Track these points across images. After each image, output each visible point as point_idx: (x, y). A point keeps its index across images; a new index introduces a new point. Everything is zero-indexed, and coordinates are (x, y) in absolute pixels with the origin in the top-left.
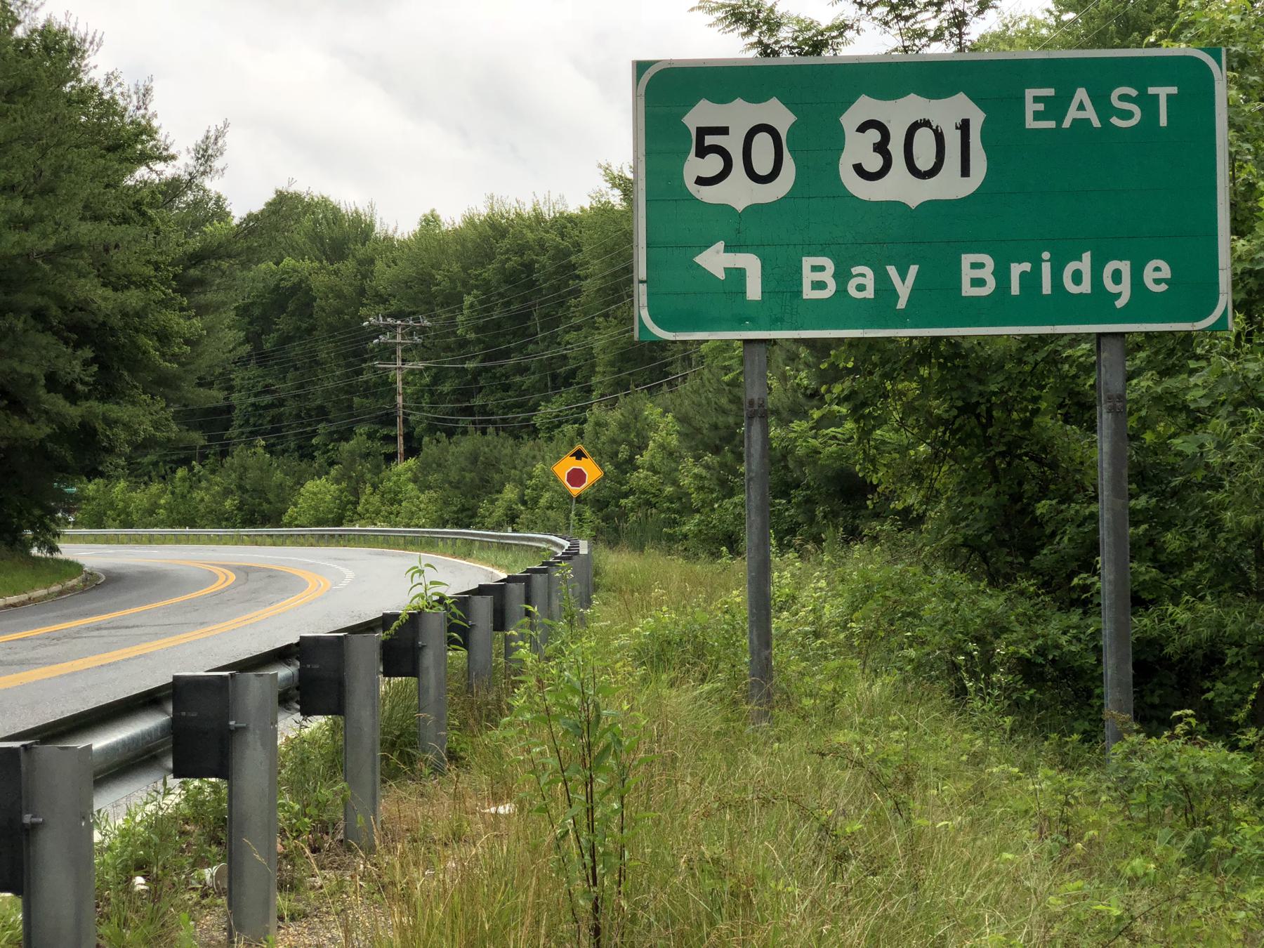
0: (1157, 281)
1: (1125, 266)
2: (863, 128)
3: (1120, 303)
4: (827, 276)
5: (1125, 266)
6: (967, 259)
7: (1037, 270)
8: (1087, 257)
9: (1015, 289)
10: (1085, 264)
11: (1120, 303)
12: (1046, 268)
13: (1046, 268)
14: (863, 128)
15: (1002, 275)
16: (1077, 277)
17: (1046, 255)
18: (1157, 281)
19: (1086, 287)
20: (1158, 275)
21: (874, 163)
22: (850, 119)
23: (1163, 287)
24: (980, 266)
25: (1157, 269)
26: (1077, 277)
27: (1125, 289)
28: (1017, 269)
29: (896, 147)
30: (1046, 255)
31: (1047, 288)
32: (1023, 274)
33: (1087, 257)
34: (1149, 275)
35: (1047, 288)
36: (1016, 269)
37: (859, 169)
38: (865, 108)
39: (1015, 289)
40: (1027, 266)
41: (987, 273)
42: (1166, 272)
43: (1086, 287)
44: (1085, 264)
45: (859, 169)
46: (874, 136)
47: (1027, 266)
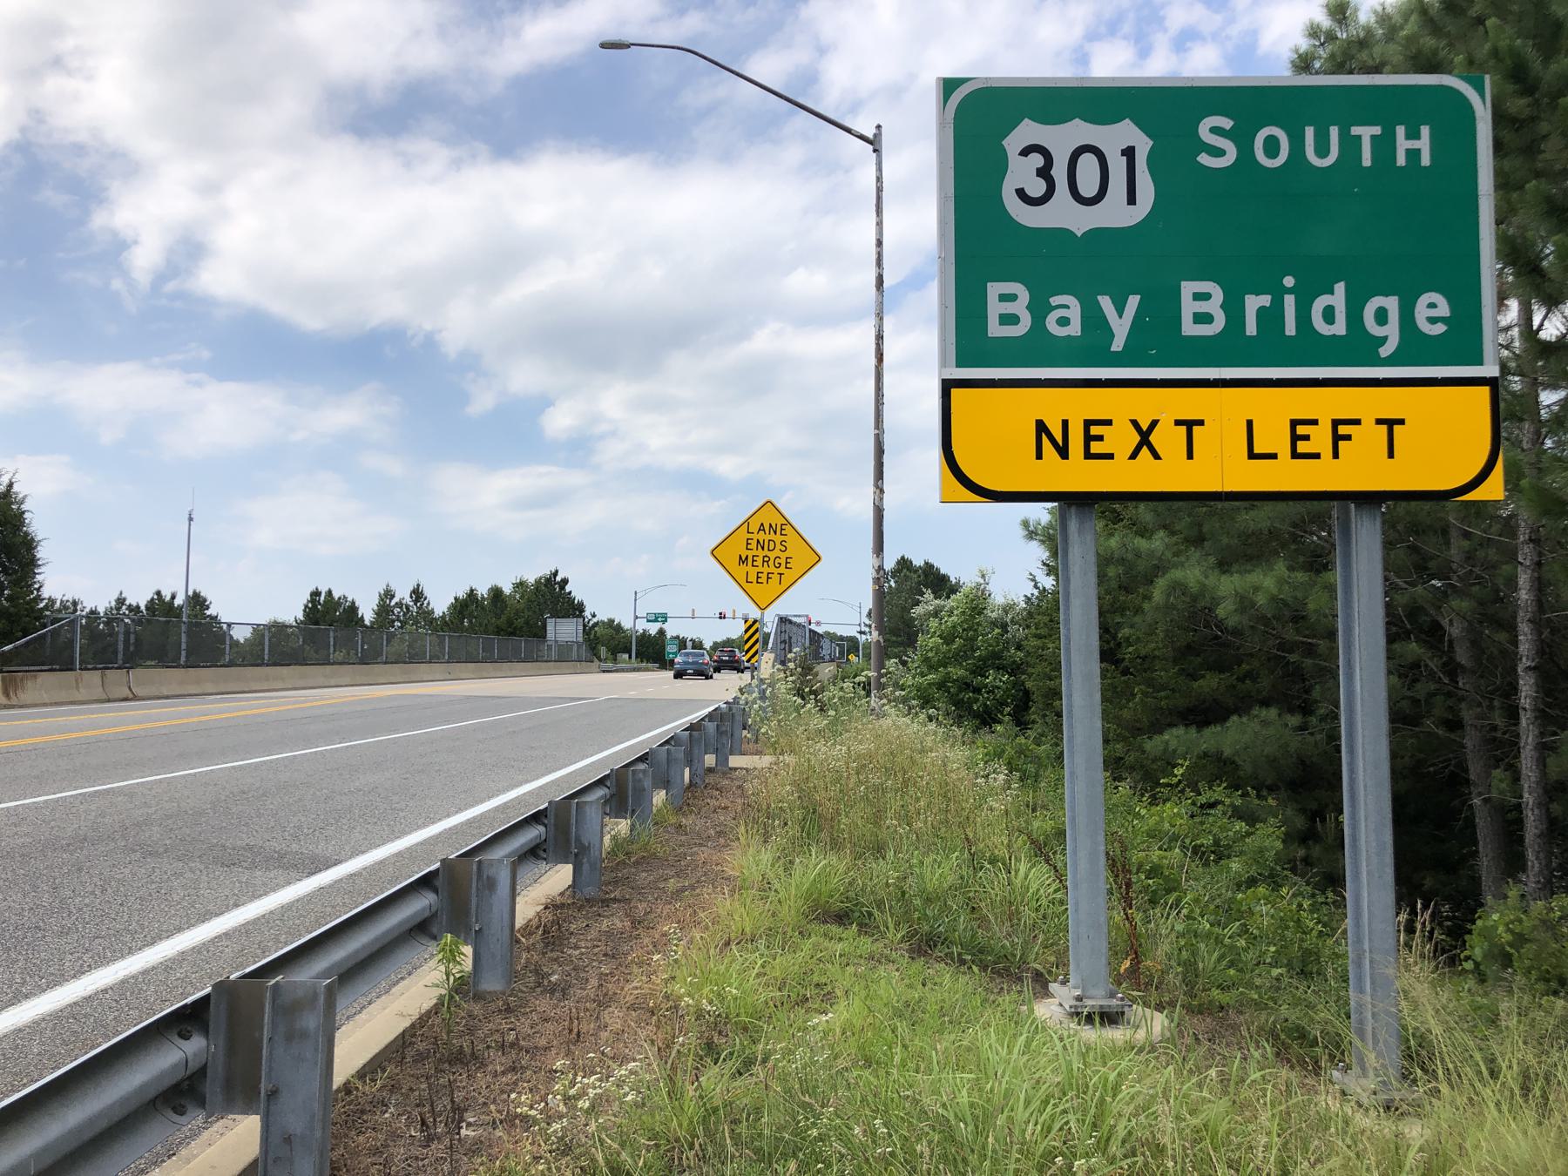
0: (1433, 320)
1: (1392, 304)
2: (1025, 152)
3: (1385, 352)
5: (1392, 304)
7: (1278, 304)
8: (1340, 288)
9: (1251, 328)
10: (1338, 298)
11: (1385, 352)
12: (1289, 301)
13: (1289, 301)
14: (1025, 152)
16: (1329, 315)
18: (1433, 320)
19: (1340, 328)
21: (1037, 188)
22: (1014, 142)
23: (1440, 329)
24: (1205, 297)
25: (1432, 306)
26: (1329, 315)
27: (1392, 331)
28: (1254, 303)
29: (1059, 172)
30: (1289, 281)
31: (1290, 329)
32: (1261, 311)
33: (1340, 288)
34: (1421, 313)
35: (1290, 329)
36: (1254, 303)
37: (1021, 193)
38: (1028, 132)
39: (1251, 328)
40: (1265, 300)
41: (1214, 306)
43: (1340, 328)
44: (1338, 298)
45: (1021, 193)
46: (1037, 160)
47: (1265, 300)
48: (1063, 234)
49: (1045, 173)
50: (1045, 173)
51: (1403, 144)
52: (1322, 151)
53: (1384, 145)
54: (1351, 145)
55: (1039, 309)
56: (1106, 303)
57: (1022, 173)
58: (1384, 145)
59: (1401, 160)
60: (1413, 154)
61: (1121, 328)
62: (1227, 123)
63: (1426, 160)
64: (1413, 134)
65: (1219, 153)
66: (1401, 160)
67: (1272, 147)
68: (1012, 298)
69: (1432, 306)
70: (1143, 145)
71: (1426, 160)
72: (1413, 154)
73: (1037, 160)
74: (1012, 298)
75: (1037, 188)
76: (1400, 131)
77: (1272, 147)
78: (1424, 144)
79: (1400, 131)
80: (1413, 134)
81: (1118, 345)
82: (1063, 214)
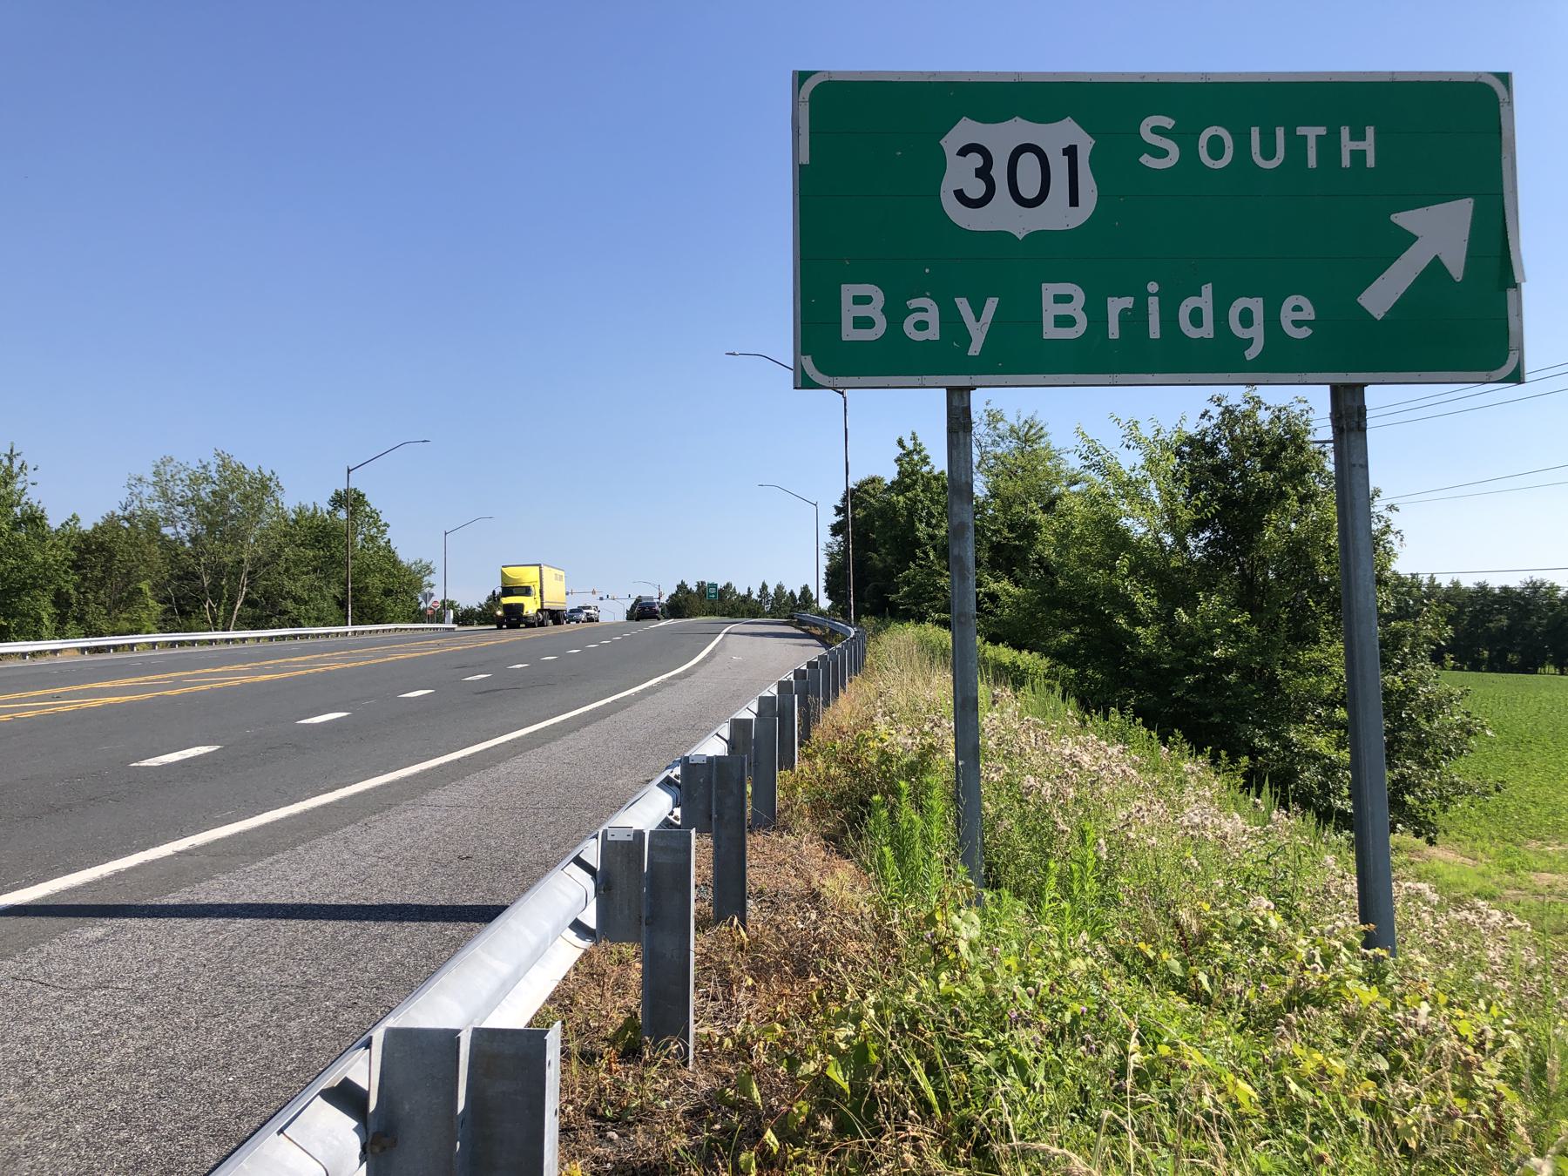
0: (1298, 324)
1: (1256, 305)
2: (964, 152)
3: (1251, 354)
4: (875, 310)
5: (1256, 305)
6: (1049, 290)
7: (1141, 309)
8: (1207, 290)
9: (1114, 331)
10: (1205, 300)
11: (1251, 354)
12: (1154, 304)
13: (1154, 304)
14: (964, 152)
15: (1096, 312)
16: (1196, 318)
17: (1153, 287)
18: (1298, 324)
19: (1207, 331)
20: (1299, 316)
21: (976, 189)
22: (952, 142)
23: (1304, 333)
25: (1297, 309)
26: (1196, 318)
27: (1257, 332)
28: (1116, 306)
29: (999, 173)
30: (1153, 287)
31: (1155, 332)
33: (1207, 290)
34: (1287, 316)
35: (1155, 332)
36: (1116, 306)
37: (960, 195)
38: (966, 131)
39: (1114, 331)
40: (1128, 302)
41: (1076, 309)
42: (1309, 313)
43: (1207, 331)
44: (1205, 300)
45: (960, 195)
46: (976, 160)
47: (1128, 302)
48: (1006, 236)
49: (984, 173)
50: (984, 173)
51: (1347, 145)
52: (1268, 153)
53: (1329, 146)
54: (1296, 146)
55: (895, 312)
56: (963, 304)
57: (960, 174)
58: (1329, 146)
59: (1346, 162)
60: (1359, 156)
61: (978, 333)
62: (1168, 122)
63: (1371, 162)
64: (1358, 135)
65: (1161, 153)
66: (1346, 162)
67: (1216, 148)
68: (867, 300)
69: (1297, 309)
70: (1085, 145)
71: (1371, 162)
72: (1359, 156)
73: (976, 160)
74: (867, 300)
75: (976, 189)
76: (1345, 132)
77: (1216, 148)
78: (1368, 145)
79: (1345, 132)
80: (1358, 135)
81: (975, 349)
82: (1002, 216)
